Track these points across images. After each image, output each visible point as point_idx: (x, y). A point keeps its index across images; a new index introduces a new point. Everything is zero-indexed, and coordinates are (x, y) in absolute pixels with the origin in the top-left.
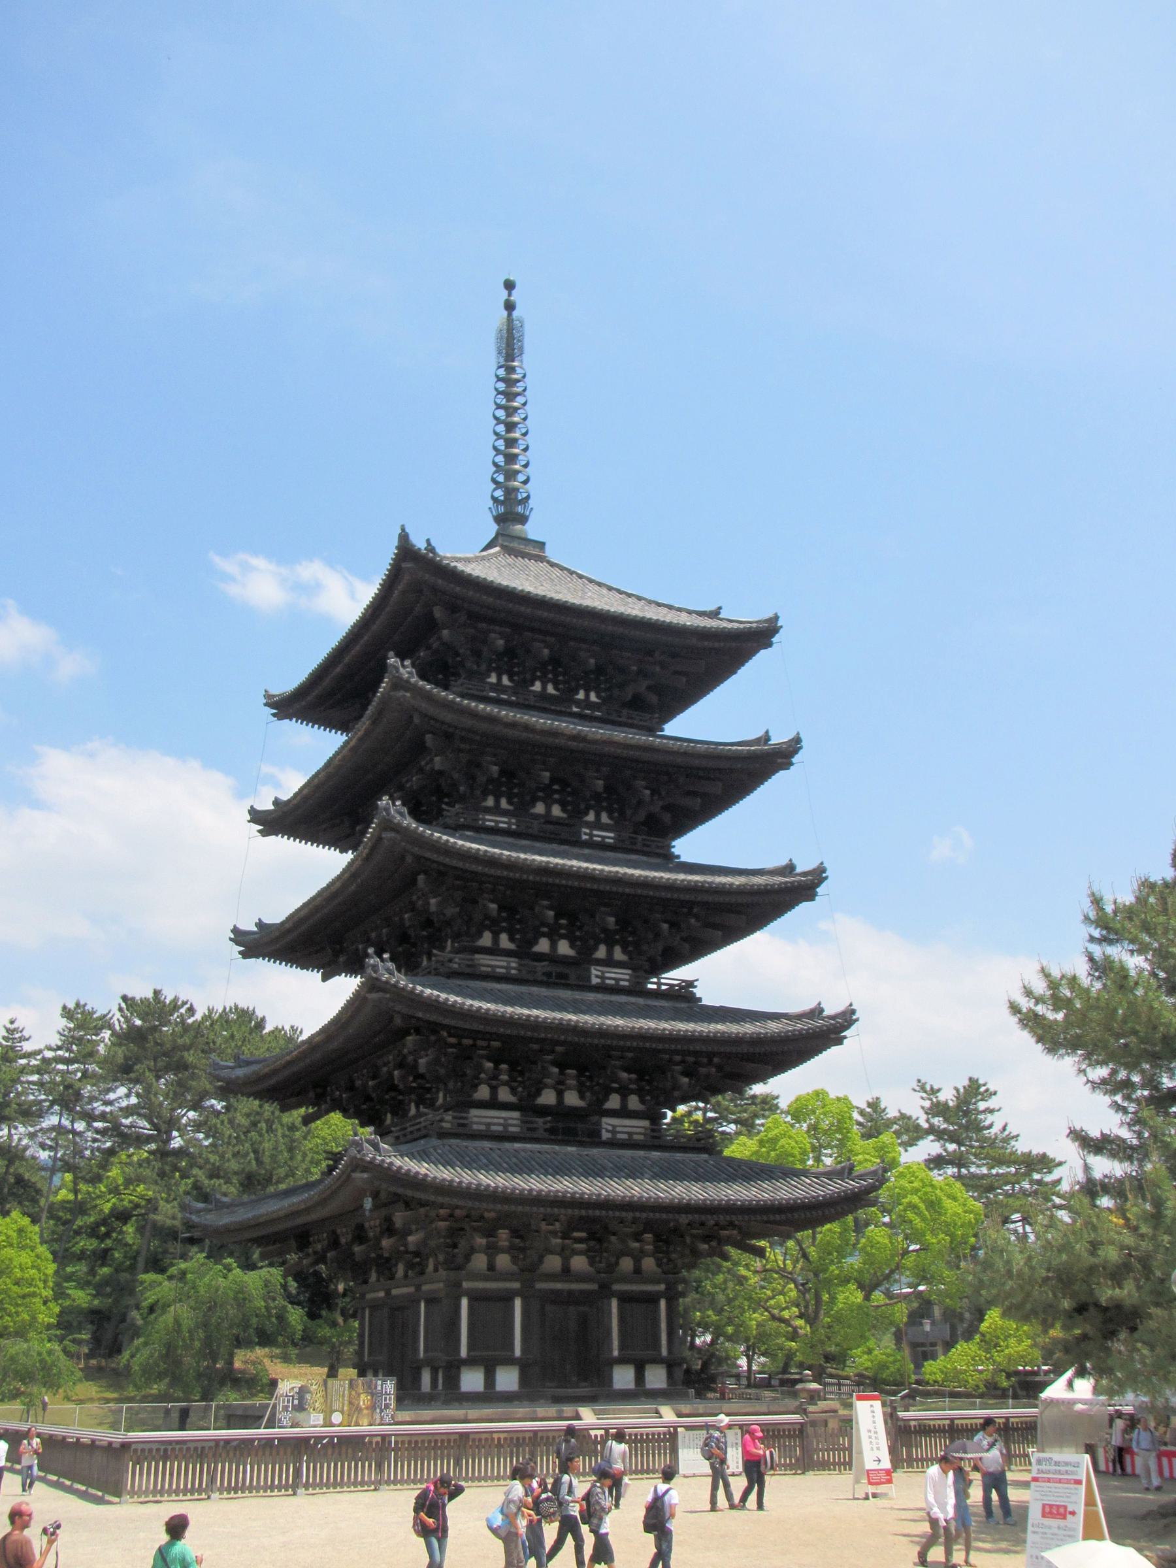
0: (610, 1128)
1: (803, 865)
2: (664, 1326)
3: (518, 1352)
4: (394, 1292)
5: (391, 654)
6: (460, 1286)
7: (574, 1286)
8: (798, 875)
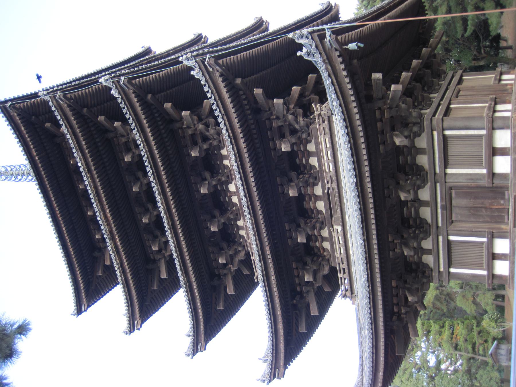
3: (485, 240)
6: (442, 272)
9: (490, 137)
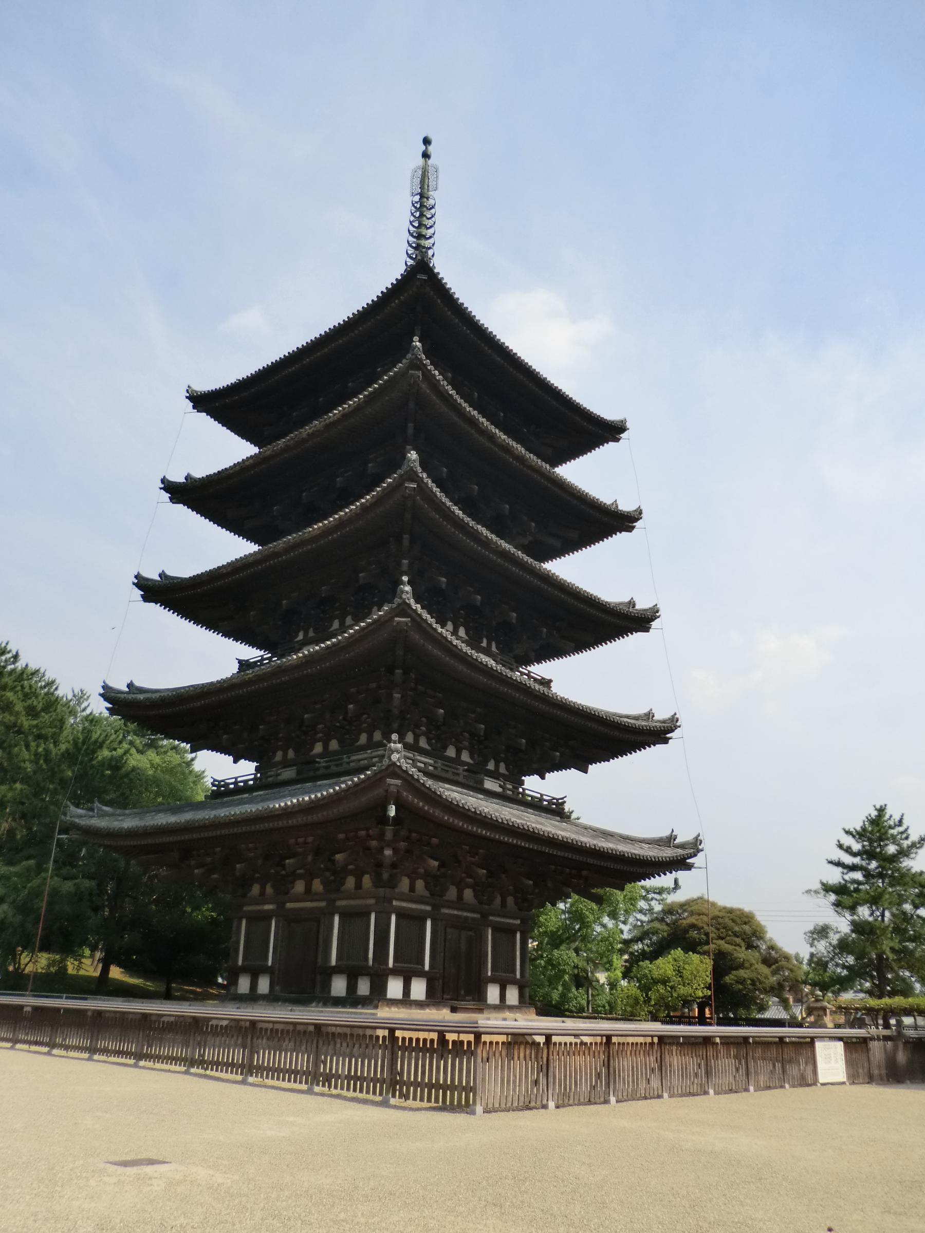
0: (502, 784)
1: (642, 604)
2: (518, 953)
3: (427, 968)
4: (289, 905)
5: (416, 338)
6: (392, 902)
7: (465, 914)
8: (637, 610)
9: (514, 982)
